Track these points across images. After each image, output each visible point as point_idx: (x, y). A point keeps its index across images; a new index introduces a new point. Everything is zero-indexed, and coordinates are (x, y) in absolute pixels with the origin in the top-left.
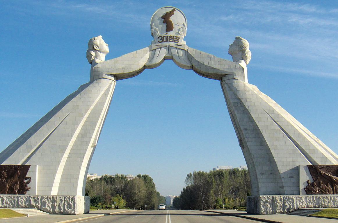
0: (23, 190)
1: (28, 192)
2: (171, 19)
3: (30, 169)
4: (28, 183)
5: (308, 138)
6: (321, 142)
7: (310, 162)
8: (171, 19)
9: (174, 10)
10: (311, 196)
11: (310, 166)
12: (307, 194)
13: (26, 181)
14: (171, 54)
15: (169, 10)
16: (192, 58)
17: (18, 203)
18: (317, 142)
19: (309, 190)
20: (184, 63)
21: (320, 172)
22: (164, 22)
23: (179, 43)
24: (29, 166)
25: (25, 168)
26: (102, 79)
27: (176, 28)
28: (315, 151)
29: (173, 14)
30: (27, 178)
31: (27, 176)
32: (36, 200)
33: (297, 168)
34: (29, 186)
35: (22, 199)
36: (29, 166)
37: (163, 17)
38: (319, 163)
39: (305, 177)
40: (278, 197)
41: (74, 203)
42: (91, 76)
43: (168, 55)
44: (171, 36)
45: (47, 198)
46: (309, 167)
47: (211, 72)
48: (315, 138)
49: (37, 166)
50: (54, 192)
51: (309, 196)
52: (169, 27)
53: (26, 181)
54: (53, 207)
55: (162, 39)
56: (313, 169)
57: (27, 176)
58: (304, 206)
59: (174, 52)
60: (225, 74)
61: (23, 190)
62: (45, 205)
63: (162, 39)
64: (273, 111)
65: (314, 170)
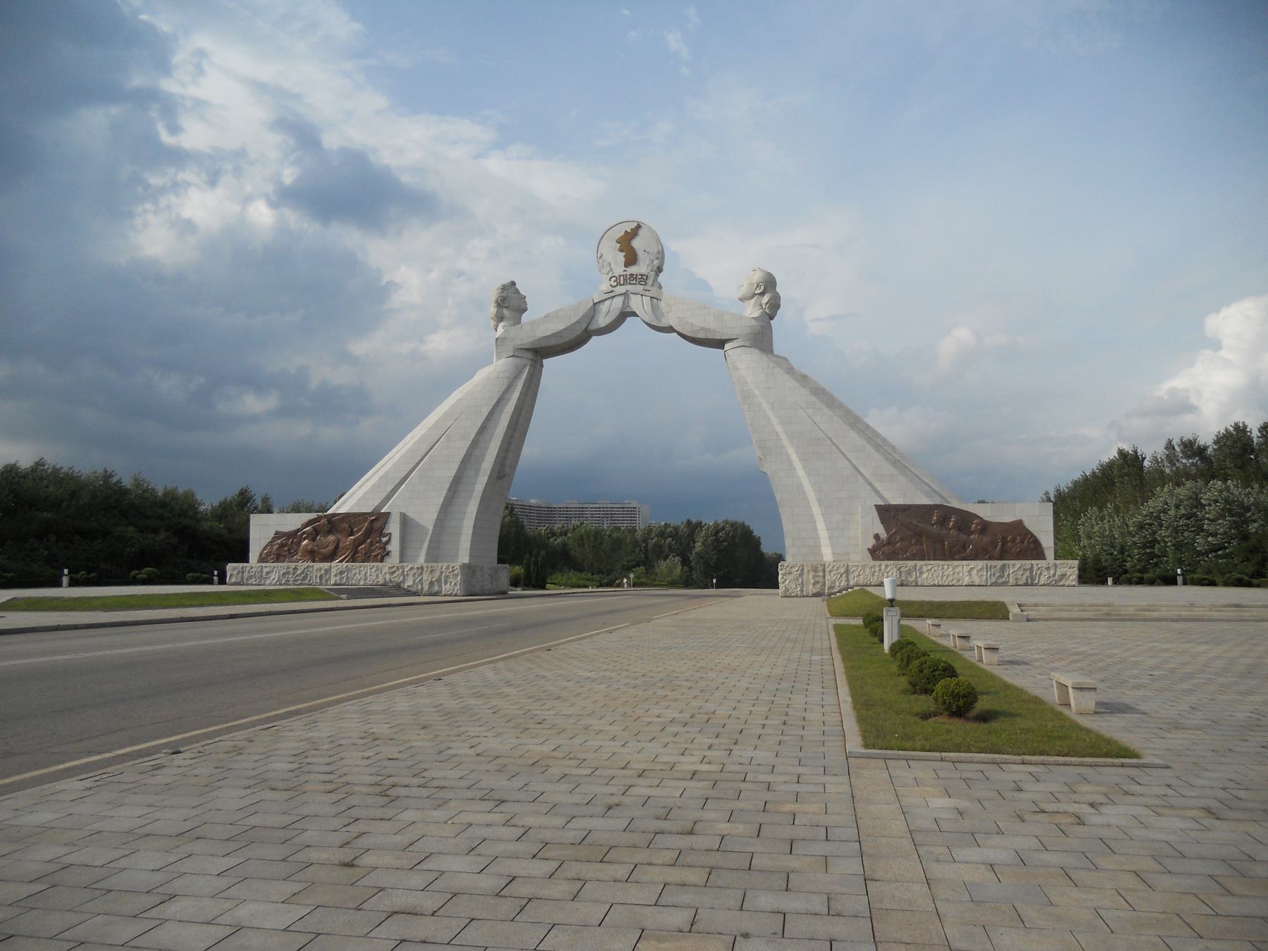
2: (636, 243)
4: (388, 542)
8: (636, 243)
9: (639, 227)
13: (384, 539)
15: (629, 228)
24: (388, 515)
34: (389, 548)
39: (869, 527)
44: (632, 275)
47: (701, 335)
51: (877, 563)
53: (384, 539)
56: (887, 513)
57: (386, 531)
65: (887, 513)
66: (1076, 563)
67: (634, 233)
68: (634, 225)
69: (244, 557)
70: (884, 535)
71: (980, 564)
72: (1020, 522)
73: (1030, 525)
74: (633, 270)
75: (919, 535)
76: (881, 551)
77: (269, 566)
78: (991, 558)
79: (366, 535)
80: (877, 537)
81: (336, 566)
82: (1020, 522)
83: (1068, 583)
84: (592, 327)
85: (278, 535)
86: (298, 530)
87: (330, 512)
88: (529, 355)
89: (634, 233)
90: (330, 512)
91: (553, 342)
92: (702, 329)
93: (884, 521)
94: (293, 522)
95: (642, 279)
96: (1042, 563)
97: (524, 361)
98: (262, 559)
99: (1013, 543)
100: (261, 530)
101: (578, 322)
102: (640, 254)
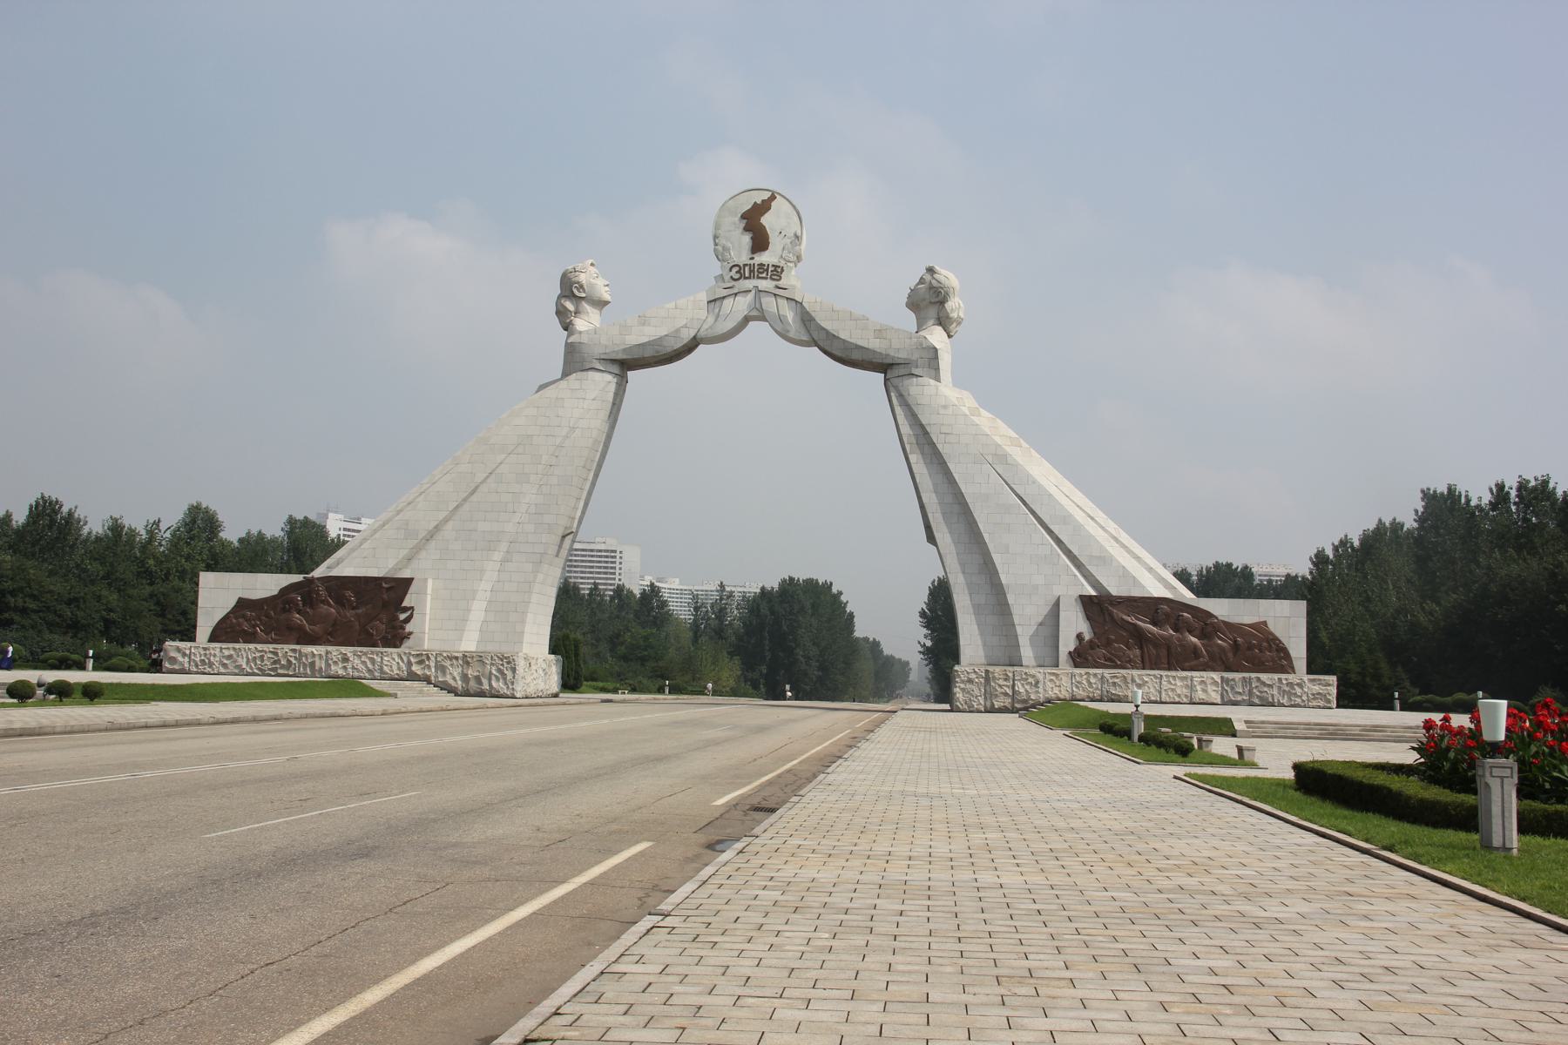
0: (395, 636)
1: (407, 643)
2: (766, 220)
3: (413, 588)
5: (1091, 528)
6: (1124, 537)
7: (1094, 587)
8: (766, 220)
9: (773, 198)
10: (1083, 671)
11: (1090, 597)
12: (1076, 666)
13: (403, 616)
14: (761, 310)
16: (812, 319)
17: (381, 669)
18: (1116, 540)
19: (1081, 657)
20: (791, 335)
21: (1111, 614)
22: (746, 229)
23: (781, 283)
24: (409, 581)
25: (401, 586)
26: (591, 373)
27: (776, 243)
28: (1105, 559)
29: (769, 208)
30: (406, 609)
31: (405, 604)
32: (422, 659)
33: (1057, 604)
34: (409, 628)
35: (391, 659)
36: (409, 581)
37: (744, 217)
38: (1114, 591)
39: (1074, 625)
40: (998, 669)
41: (514, 670)
42: (566, 362)
43: (755, 313)
44: (761, 265)
45: (450, 658)
46: (1086, 601)
47: (856, 356)
48: (1112, 526)
49: (430, 582)
50: (469, 644)
51: (1078, 671)
52: (760, 242)
53: (403, 616)
54: (465, 678)
55: (741, 272)
56: (1098, 606)
57: (405, 604)
58: (1064, 694)
59: (769, 304)
60: (889, 361)
61: (395, 636)
62: (444, 673)
63: (741, 272)
64: (1003, 458)
65: (1098, 606)
66: (1333, 679)
67: (764, 207)
68: (766, 195)
69: (188, 634)
70: (1087, 637)
71: (1216, 676)
72: (1265, 623)
73: (1276, 629)
74: (765, 258)
75: (1140, 637)
76: (1081, 657)
77: (228, 648)
78: (1228, 669)
79: (375, 611)
80: (1079, 637)
81: (335, 651)
82: (1265, 623)
83: (1322, 703)
84: (702, 334)
85: (242, 604)
86: (274, 597)
87: (318, 573)
88: (616, 369)
89: (762, 208)
90: (318, 573)
91: (648, 353)
92: (858, 347)
93: (1089, 618)
94: (266, 585)
95: (777, 272)
96: (1291, 677)
97: (609, 377)
98: (214, 638)
99: (1254, 652)
100: (218, 594)
101: (685, 326)
102: (775, 240)
